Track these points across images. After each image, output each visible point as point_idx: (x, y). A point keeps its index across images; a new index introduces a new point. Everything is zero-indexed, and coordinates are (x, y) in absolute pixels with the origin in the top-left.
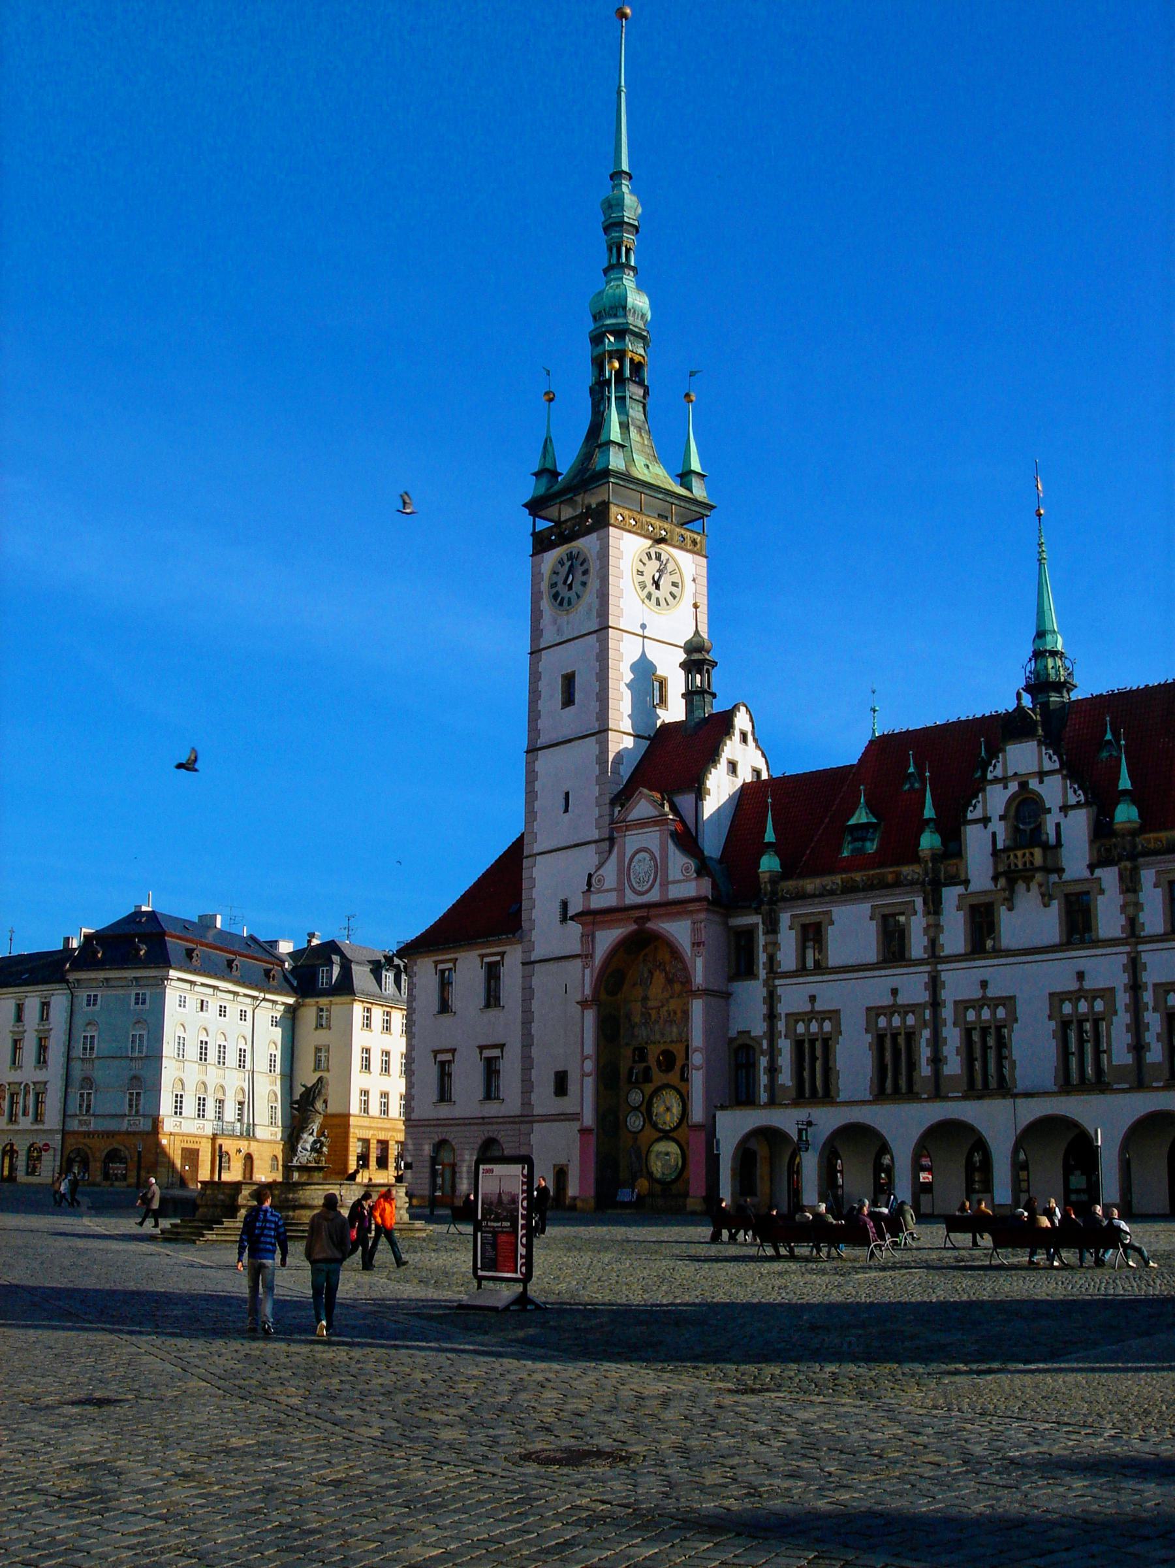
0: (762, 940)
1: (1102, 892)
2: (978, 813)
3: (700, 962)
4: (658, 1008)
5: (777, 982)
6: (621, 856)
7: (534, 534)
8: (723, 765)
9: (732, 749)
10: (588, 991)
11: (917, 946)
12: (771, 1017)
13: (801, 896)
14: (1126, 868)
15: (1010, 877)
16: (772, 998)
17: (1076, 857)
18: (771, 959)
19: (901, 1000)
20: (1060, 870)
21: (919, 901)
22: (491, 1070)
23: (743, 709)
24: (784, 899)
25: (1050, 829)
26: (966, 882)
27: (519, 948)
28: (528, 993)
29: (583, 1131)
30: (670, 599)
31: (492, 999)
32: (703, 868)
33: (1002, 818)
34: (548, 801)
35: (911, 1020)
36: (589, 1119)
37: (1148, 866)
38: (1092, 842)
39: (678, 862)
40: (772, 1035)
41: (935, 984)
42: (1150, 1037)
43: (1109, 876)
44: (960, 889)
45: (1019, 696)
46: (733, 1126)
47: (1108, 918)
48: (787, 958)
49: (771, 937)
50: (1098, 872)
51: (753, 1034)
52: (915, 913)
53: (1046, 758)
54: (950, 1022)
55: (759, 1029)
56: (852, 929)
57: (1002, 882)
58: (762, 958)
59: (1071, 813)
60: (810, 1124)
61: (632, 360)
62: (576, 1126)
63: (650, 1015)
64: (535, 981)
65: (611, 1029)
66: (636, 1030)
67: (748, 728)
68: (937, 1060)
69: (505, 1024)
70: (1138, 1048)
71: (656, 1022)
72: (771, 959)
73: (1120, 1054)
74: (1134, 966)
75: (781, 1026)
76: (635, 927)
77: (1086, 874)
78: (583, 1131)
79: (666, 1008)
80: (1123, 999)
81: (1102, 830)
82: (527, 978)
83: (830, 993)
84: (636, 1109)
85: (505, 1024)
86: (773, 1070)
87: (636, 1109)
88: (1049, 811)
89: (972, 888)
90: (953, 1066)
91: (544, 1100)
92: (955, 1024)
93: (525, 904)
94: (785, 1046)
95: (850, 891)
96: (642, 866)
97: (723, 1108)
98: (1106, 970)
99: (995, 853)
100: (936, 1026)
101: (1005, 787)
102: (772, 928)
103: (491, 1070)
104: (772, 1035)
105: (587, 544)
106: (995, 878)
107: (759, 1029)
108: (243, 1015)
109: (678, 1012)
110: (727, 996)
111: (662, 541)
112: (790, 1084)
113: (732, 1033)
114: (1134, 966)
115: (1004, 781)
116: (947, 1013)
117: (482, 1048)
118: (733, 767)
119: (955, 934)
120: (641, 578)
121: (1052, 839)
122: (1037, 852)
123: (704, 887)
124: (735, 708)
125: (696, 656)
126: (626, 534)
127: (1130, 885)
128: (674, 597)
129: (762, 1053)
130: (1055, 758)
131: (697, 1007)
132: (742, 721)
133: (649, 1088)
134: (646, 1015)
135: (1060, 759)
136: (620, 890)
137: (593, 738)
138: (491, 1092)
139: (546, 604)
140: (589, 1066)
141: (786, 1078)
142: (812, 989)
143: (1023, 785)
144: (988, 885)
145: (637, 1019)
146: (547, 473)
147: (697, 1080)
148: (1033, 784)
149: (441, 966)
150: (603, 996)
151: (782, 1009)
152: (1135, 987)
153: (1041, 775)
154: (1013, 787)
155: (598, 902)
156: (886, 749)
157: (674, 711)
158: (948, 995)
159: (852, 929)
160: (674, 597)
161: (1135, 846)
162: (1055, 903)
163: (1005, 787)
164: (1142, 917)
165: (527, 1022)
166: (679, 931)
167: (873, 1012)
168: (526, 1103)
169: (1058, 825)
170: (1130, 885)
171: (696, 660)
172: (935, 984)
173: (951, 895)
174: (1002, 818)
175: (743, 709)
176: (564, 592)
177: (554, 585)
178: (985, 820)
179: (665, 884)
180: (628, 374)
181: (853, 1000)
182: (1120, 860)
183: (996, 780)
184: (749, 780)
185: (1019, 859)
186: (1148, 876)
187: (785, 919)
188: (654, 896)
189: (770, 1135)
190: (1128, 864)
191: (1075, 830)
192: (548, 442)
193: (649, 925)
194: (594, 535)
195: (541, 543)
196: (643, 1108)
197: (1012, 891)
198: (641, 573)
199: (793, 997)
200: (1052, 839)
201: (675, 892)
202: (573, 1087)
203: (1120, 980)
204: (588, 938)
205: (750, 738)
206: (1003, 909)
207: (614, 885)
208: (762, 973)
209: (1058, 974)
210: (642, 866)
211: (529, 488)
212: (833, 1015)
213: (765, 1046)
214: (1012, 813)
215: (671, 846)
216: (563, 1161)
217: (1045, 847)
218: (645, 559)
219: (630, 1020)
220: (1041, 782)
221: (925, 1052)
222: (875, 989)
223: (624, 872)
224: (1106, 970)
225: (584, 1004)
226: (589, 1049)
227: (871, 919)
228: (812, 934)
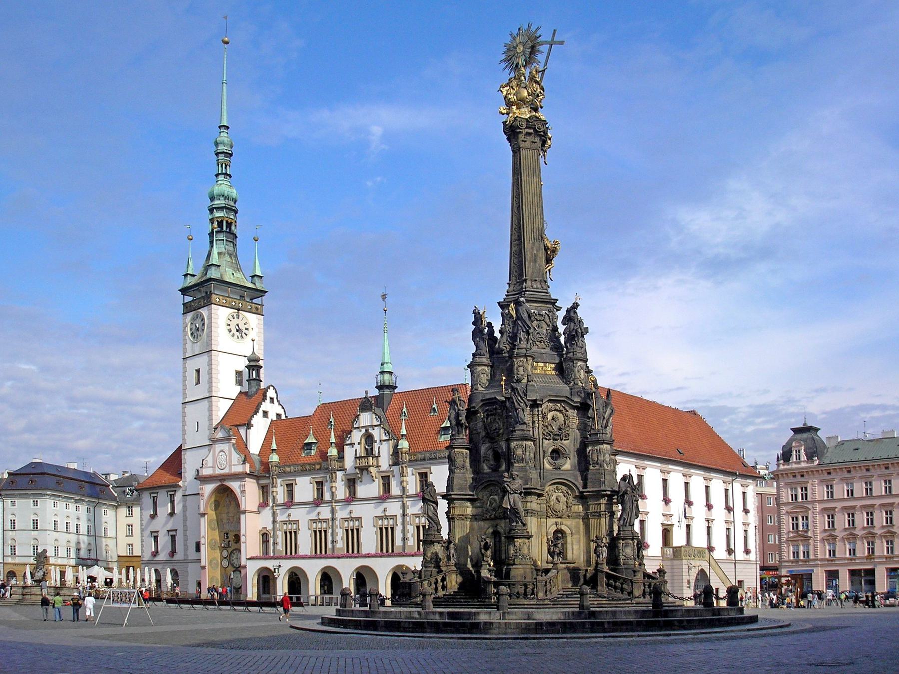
6: (214, 452)
8: (260, 413)
9: (266, 406)
17: (384, 461)
23: (271, 388)
32: (247, 458)
33: (359, 444)
39: (236, 457)
42: (409, 535)
46: (252, 570)
67: (274, 396)
70: (404, 539)
73: (398, 542)
80: (399, 520)
82: (185, 502)
94: (280, 536)
95: (303, 472)
96: (222, 457)
99: (356, 458)
118: (265, 414)
119: (341, 491)
124: (268, 388)
125: (252, 364)
132: (271, 393)
148: (370, 431)
152: (404, 515)
154: (363, 431)
155: (206, 472)
156: (325, 408)
159: (305, 488)
165: (185, 521)
171: (254, 365)
172: (333, 512)
173: (339, 474)
175: (271, 388)
178: (352, 445)
179: (230, 466)
184: (274, 418)
185: (363, 463)
188: (226, 471)
191: (384, 451)
203: (399, 513)
205: (275, 401)
208: (271, 504)
224: (393, 508)
228: (290, 488)
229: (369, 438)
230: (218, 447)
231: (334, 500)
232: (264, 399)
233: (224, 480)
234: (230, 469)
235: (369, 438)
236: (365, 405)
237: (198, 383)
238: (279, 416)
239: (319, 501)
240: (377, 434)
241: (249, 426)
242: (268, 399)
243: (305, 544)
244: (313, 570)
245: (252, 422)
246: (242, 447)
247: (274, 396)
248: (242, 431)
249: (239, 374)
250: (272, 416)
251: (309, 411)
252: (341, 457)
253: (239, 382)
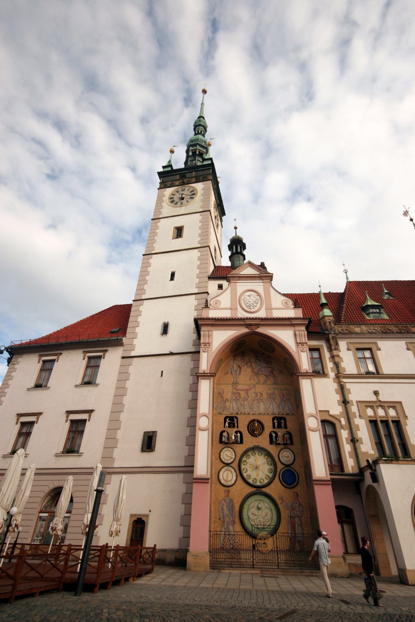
4: (247, 390)
12: (345, 402)
16: (342, 389)
22: (77, 428)
28: (123, 376)
55: (336, 410)
63: (239, 394)
64: (131, 369)
66: (228, 404)
71: (245, 399)
79: (253, 391)
84: (228, 465)
86: (354, 441)
87: (228, 465)
103: (77, 428)
107: (336, 410)
109: (264, 394)
129: (342, 427)
133: (240, 449)
138: (72, 448)
142: (376, 387)
151: (353, 397)
196: (235, 465)
201: (276, 314)
202: (160, 443)
207: (229, 306)
213: (343, 421)
219: (222, 397)
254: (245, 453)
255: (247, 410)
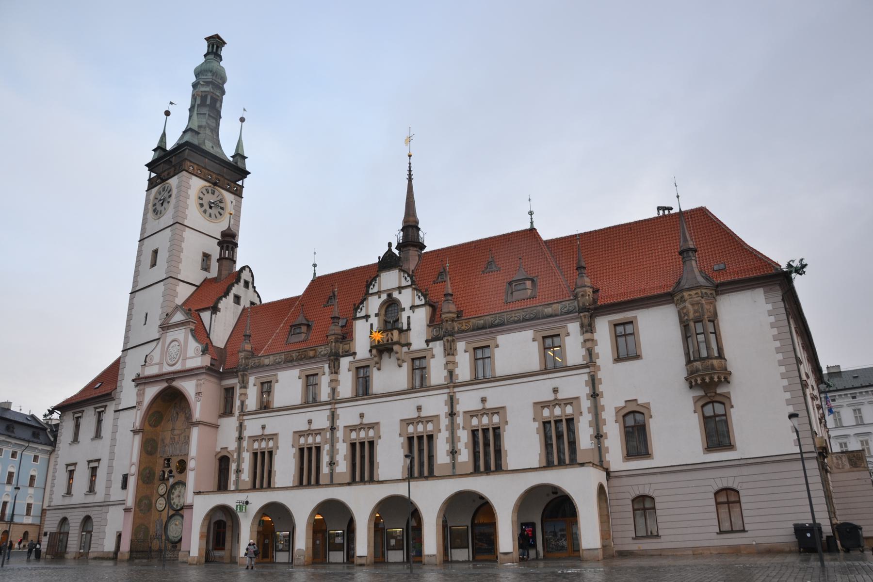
0: (238, 392)
1: (433, 356)
2: (363, 314)
3: (199, 404)
4: (179, 435)
5: (245, 418)
7: (150, 180)
8: (231, 297)
10: (138, 425)
11: (324, 394)
12: (240, 438)
13: (260, 367)
14: (448, 341)
15: (382, 350)
16: (241, 427)
17: (418, 337)
18: (243, 403)
19: (313, 427)
20: (409, 345)
21: (326, 366)
24: (252, 368)
25: (404, 320)
26: (355, 354)
27: (114, 403)
29: (127, 510)
30: (218, 215)
31: (98, 435)
33: (376, 315)
34: (139, 318)
35: (318, 439)
36: (130, 503)
37: (460, 339)
38: (429, 326)
39: (193, 346)
40: (239, 449)
41: (333, 417)
43: (438, 347)
44: (350, 358)
45: (390, 244)
46: (202, 506)
47: (437, 373)
48: (252, 403)
49: (243, 391)
50: (431, 345)
51: (229, 449)
52: (324, 374)
53: (403, 279)
54: (341, 440)
55: (232, 446)
56: (288, 385)
57: (374, 351)
58: (237, 403)
59: (417, 310)
60: (247, 503)
61: (212, 97)
62: (124, 507)
64: (119, 422)
65: (149, 448)
68: (332, 464)
69: (100, 449)
70: (453, 452)
72: (243, 403)
73: (442, 456)
74: (452, 401)
75: (245, 444)
76: (165, 385)
77: (424, 346)
78: (127, 510)
80: (444, 422)
81: (433, 321)
82: (116, 419)
83: (274, 424)
84: (162, 496)
85: (100, 449)
86: (238, 471)
87: (162, 496)
88: (404, 310)
89: (358, 357)
90: (343, 467)
91: (116, 493)
92: (344, 441)
93: (120, 378)
94: (247, 457)
95: (289, 362)
97: (199, 493)
98: (434, 404)
100: (333, 442)
101: (379, 297)
102: (244, 386)
104: (239, 449)
105: (173, 182)
106: (370, 351)
107: (232, 446)
108: (14, 455)
110: (216, 427)
111: (215, 184)
112: (247, 479)
113: (218, 450)
114: (452, 401)
115: (379, 293)
116: (340, 434)
117: (89, 462)
118: (237, 299)
119: (346, 385)
120: (201, 201)
121: (405, 327)
122: (396, 333)
123: (206, 361)
126: (194, 178)
127: (450, 351)
128: (221, 214)
130: (408, 278)
131: (195, 432)
132: (245, 275)
134: (173, 439)
135: (412, 279)
136: (160, 364)
137: (162, 283)
138: (92, 490)
139: (150, 214)
140: (134, 470)
141: (246, 476)
143: (389, 295)
144: (368, 355)
145: (167, 441)
146: (160, 148)
147: (191, 478)
148: (395, 295)
149: (77, 415)
150: (148, 428)
151: (246, 434)
152: (452, 414)
153: (400, 289)
154: (384, 297)
156: (319, 284)
157: (214, 273)
158: (341, 423)
160: (221, 214)
161: (453, 328)
162: (405, 365)
163: (379, 297)
164: (457, 371)
165: (113, 446)
166: (188, 387)
167: (300, 434)
168: (107, 494)
169: (409, 318)
170: (450, 351)
172: (333, 417)
173: (345, 362)
174: (376, 315)
175: (247, 269)
176: (159, 207)
177: (154, 205)
179: (185, 359)
180: (208, 102)
181: (285, 429)
182: (444, 336)
183: (372, 294)
186: (461, 346)
187: (252, 380)
188: (178, 367)
189: (224, 509)
190: (450, 338)
191: (418, 321)
192: (164, 135)
193: (175, 384)
194: (176, 177)
195: (152, 184)
196: (166, 496)
197: (381, 358)
198: (201, 199)
199: (253, 427)
200: (405, 327)
204: (140, 394)
205: (250, 286)
206: (375, 369)
208: (237, 411)
209: (406, 408)
210: (174, 350)
211: (150, 157)
212: (273, 437)
213: (235, 456)
214: (383, 312)
215: (190, 338)
216: (120, 529)
217: (401, 331)
218: (205, 192)
220: (400, 293)
221: (325, 459)
222: (299, 421)
223: (164, 353)
224: (434, 404)
225: (135, 432)
226: (135, 458)
227: (299, 378)
228: (266, 388)
229: (391, 305)
230: (171, 335)
231: (335, 400)
232: (238, 281)
233: (173, 379)
234: (184, 364)
235: (391, 305)
236: (388, 262)
237: (153, 265)
238: (252, 303)
239: (310, 401)
240: (406, 298)
241: (215, 309)
242: (242, 281)
243: (285, 467)
244: (302, 505)
245: (220, 306)
246: (201, 334)
247: (250, 280)
248: (206, 316)
249: (206, 257)
250: (245, 303)
251: (298, 289)
252: (347, 336)
253: (206, 268)
254: (173, 486)
255: (178, 452)
